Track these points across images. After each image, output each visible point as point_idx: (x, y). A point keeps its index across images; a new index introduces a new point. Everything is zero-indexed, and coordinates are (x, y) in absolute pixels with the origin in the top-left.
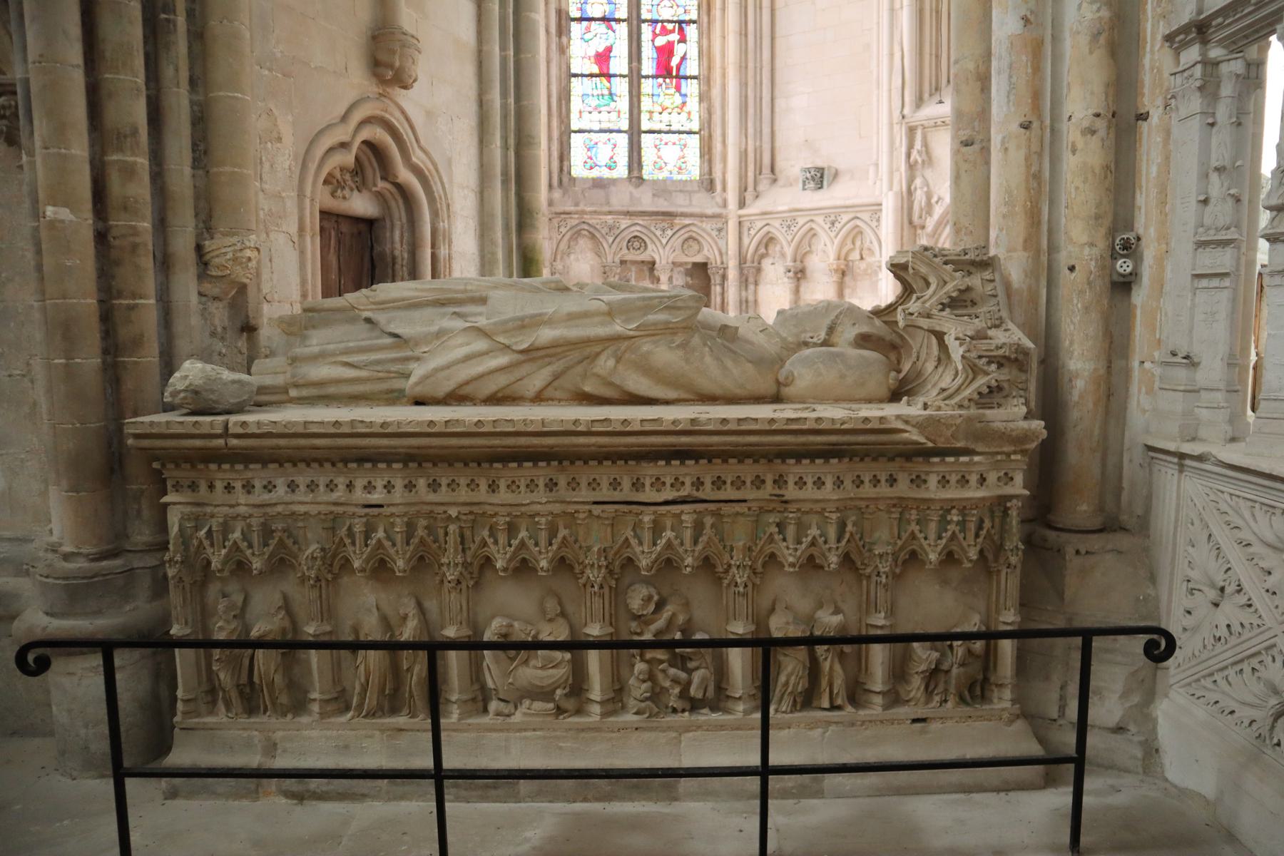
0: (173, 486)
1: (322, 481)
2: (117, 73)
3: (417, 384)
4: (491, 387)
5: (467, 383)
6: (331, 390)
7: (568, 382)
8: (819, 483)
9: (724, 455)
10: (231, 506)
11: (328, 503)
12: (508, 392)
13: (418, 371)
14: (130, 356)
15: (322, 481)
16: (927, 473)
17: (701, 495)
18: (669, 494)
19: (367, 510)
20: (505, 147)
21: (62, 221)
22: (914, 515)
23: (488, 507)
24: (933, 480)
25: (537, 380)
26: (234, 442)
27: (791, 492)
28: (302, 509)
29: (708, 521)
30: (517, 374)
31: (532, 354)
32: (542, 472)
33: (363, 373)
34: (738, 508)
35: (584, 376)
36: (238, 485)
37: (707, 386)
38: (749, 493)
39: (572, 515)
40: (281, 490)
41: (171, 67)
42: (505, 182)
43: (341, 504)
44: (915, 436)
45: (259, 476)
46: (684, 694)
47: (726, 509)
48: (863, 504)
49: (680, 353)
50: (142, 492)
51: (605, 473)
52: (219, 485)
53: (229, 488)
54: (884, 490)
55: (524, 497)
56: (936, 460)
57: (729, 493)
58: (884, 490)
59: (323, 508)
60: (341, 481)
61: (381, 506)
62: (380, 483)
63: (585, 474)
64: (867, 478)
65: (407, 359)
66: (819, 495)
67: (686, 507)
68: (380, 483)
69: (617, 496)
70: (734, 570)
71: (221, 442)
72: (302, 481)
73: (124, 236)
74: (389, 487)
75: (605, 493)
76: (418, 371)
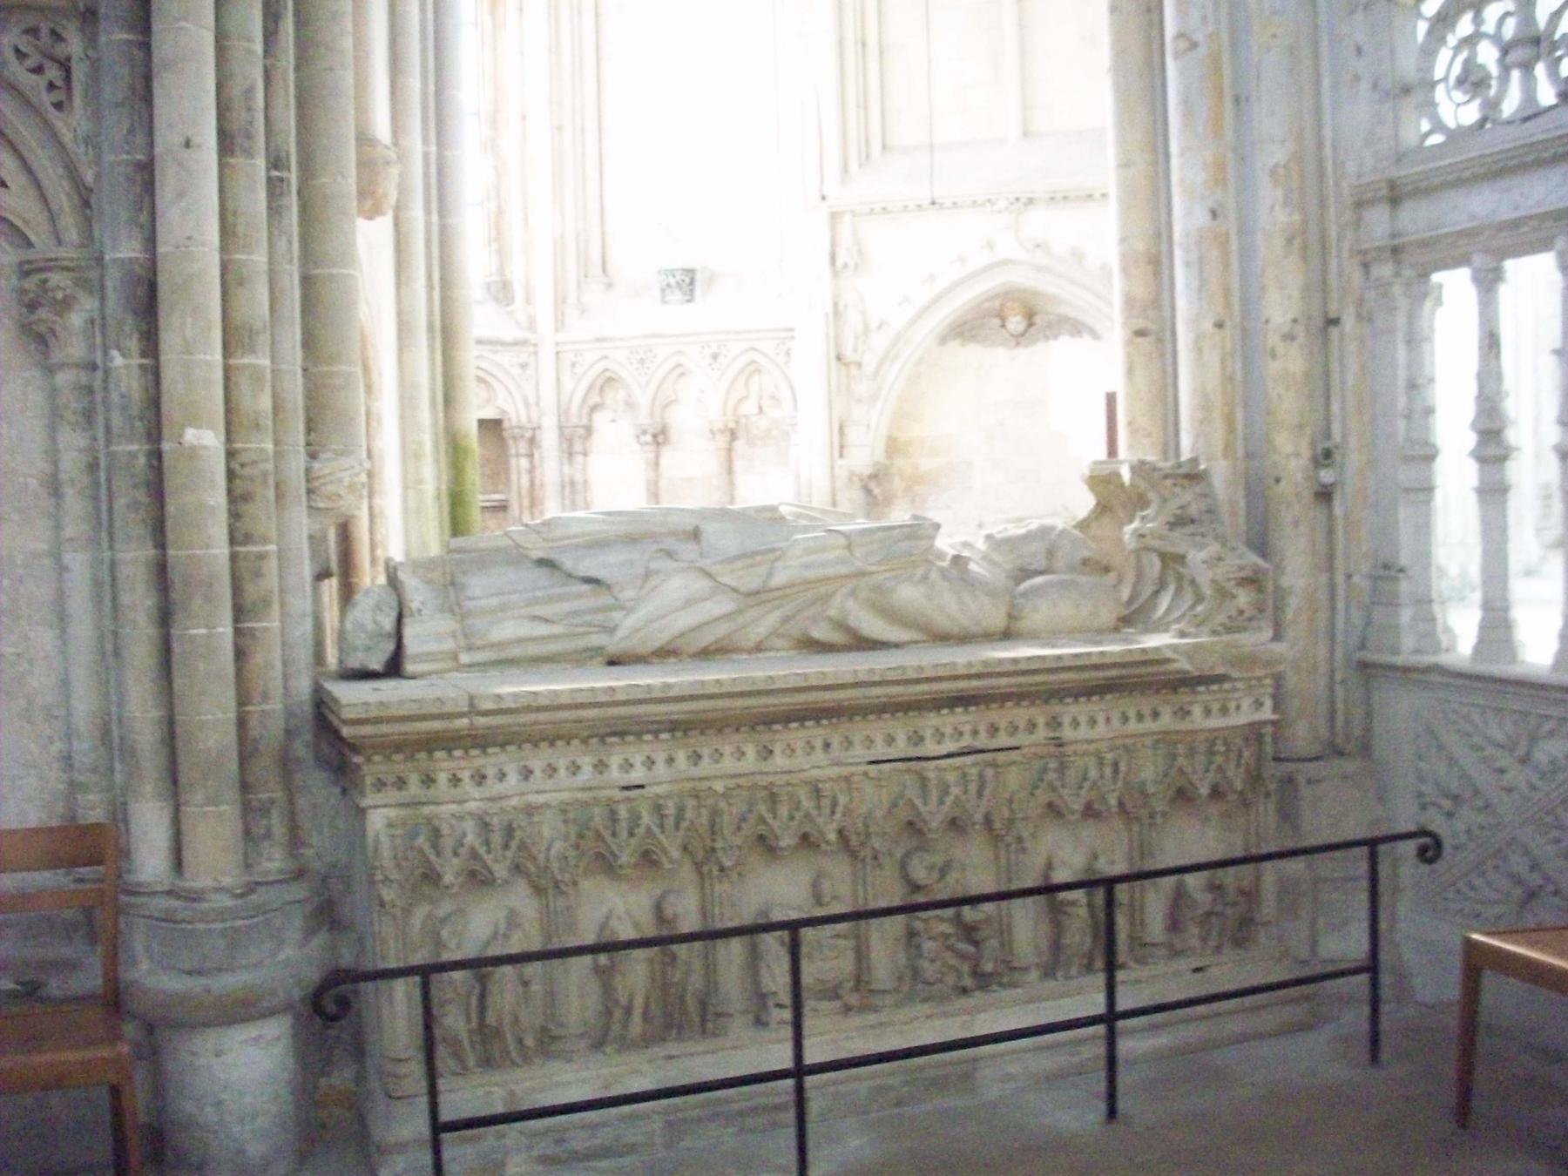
0: (374, 785)
1: (562, 764)
2: (249, 254)
3: (623, 639)
4: (707, 638)
5: (682, 635)
6: (516, 652)
7: (794, 629)
8: (1093, 722)
9: (1003, 698)
10: (460, 802)
11: (570, 790)
12: (670, 647)
13: (628, 623)
14: (260, 621)
15: (562, 764)
16: (1191, 703)
17: (978, 744)
18: (949, 746)
19: (627, 793)
20: (430, 287)
21: (205, 448)
22: (1181, 749)
23: (758, 778)
24: (1197, 711)
25: (764, 624)
26: (481, 721)
27: (1067, 733)
28: (541, 799)
29: (989, 772)
30: (740, 620)
31: (757, 597)
32: (816, 733)
33: (558, 629)
34: (1014, 755)
35: (814, 621)
36: (465, 775)
37: (942, 623)
38: (1021, 739)
39: (847, 779)
40: (513, 779)
41: (284, 238)
42: (431, 338)
43: (590, 789)
44: (1183, 665)
45: (491, 761)
46: (977, 974)
47: (1001, 757)
48: (1128, 741)
49: (922, 589)
50: (272, 801)
51: (877, 729)
52: (443, 778)
53: (455, 781)
54: (1149, 725)
55: (800, 761)
56: (1202, 689)
57: (1003, 740)
58: (1149, 725)
59: (566, 796)
60: (587, 762)
61: (641, 787)
62: (638, 760)
63: (859, 729)
64: (1132, 714)
65: (610, 608)
66: (1093, 734)
67: (968, 760)
68: (638, 760)
69: (893, 753)
70: (1018, 824)
71: (465, 721)
72: (537, 765)
73: (254, 462)
74: (650, 763)
75: (880, 751)
76: (628, 623)
